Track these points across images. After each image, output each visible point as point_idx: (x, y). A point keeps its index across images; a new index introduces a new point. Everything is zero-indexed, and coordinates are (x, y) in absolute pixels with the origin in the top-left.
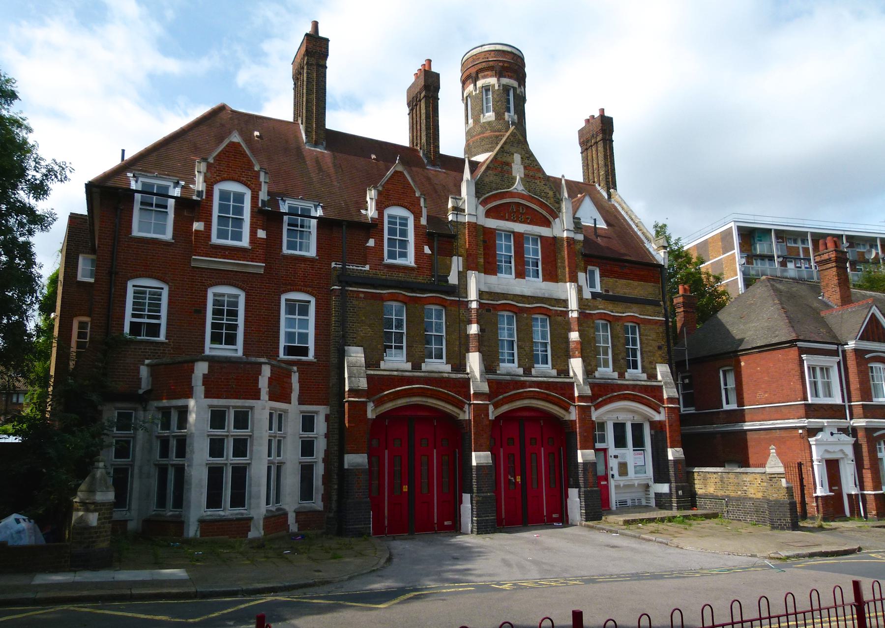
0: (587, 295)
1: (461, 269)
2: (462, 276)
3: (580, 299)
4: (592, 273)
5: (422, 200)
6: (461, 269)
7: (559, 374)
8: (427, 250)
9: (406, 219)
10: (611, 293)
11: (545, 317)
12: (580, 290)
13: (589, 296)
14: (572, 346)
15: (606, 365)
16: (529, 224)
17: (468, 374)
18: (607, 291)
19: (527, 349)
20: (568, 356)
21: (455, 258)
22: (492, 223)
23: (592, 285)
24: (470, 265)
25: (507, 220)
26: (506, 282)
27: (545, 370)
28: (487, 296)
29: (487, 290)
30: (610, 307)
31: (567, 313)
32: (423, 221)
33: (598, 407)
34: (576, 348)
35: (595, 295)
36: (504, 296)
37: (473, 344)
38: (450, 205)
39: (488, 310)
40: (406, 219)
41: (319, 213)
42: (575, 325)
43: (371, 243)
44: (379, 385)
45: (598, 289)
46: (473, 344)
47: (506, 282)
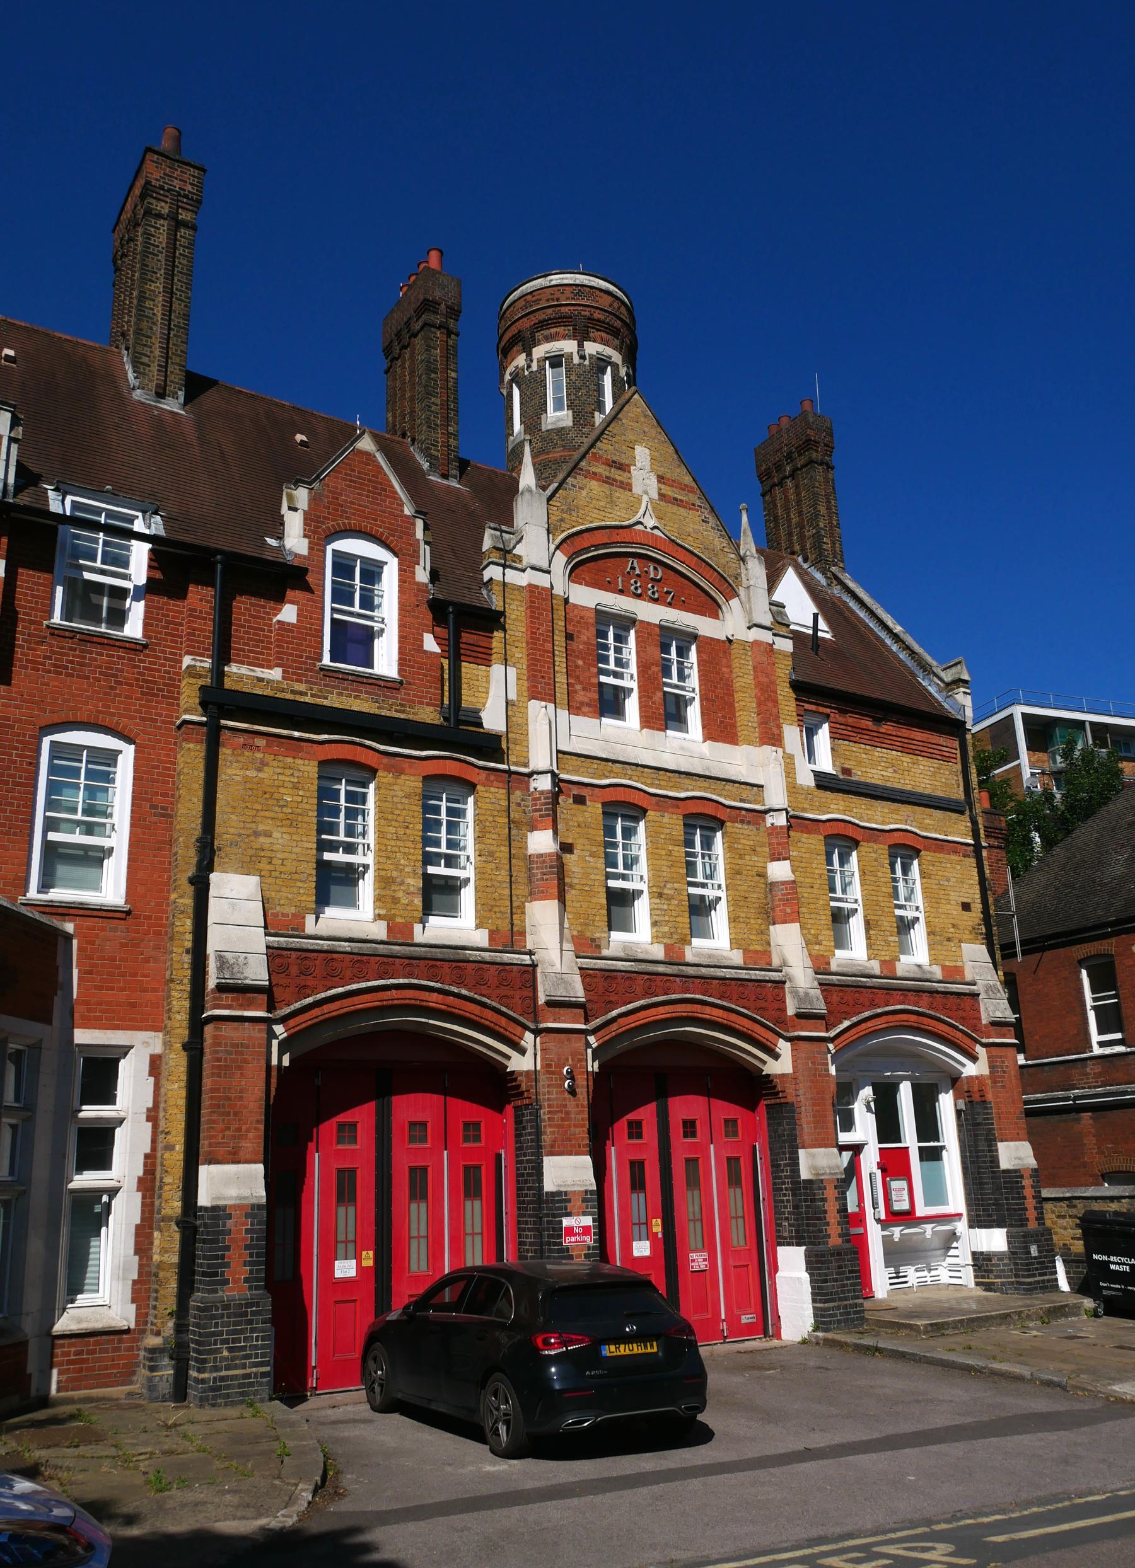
1: (512, 696)
3: (793, 788)
5: (419, 524)
6: (512, 696)
8: (430, 644)
9: (380, 565)
16: (670, 605)
17: (531, 953)
21: (497, 670)
22: (586, 597)
24: (539, 686)
25: (621, 592)
26: (626, 735)
32: (422, 575)
38: (487, 544)
40: (380, 565)
41: (157, 526)
43: (288, 613)
44: (294, 963)
47: (626, 735)
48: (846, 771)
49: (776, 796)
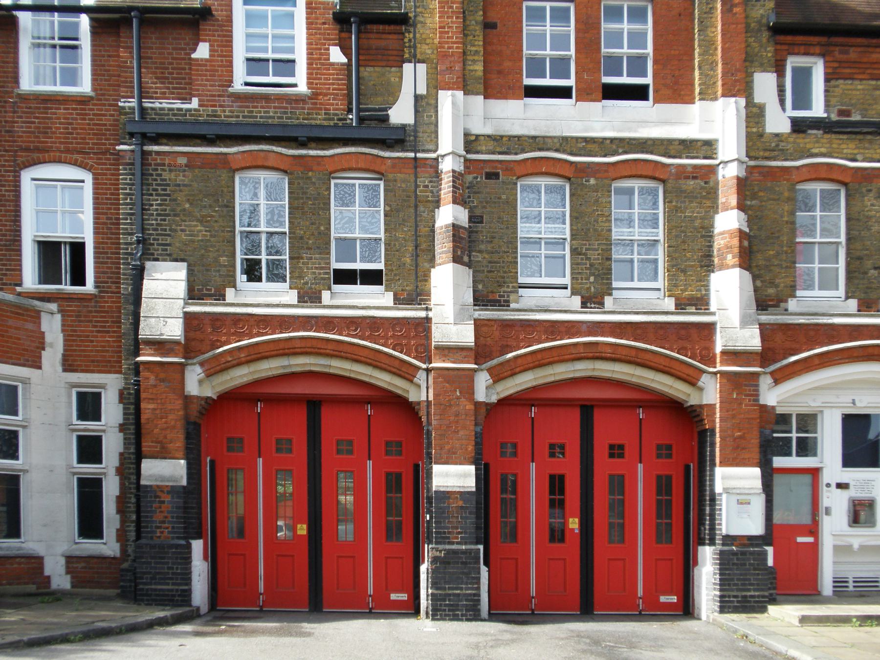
0: (778, 122)
2: (424, 105)
4: (803, 77)
7: (681, 306)
10: (856, 117)
11: (651, 184)
12: (755, 115)
13: (785, 127)
14: (719, 243)
15: (828, 283)
18: (841, 113)
19: (593, 255)
20: (707, 263)
23: (802, 99)
27: (642, 296)
28: (491, 145)
29: (488, 130)
30: (849, 147)
31: (712, 170)
33: (779, 378)
34: (729, 247)
35: (799, 126)
36: (536, 142)
37: (443, 246)
39: (492, 176)
42: (728, 196)
45: (818, 110)
46: (443, 246)
48: (847, 113)
49: (730, 151)
